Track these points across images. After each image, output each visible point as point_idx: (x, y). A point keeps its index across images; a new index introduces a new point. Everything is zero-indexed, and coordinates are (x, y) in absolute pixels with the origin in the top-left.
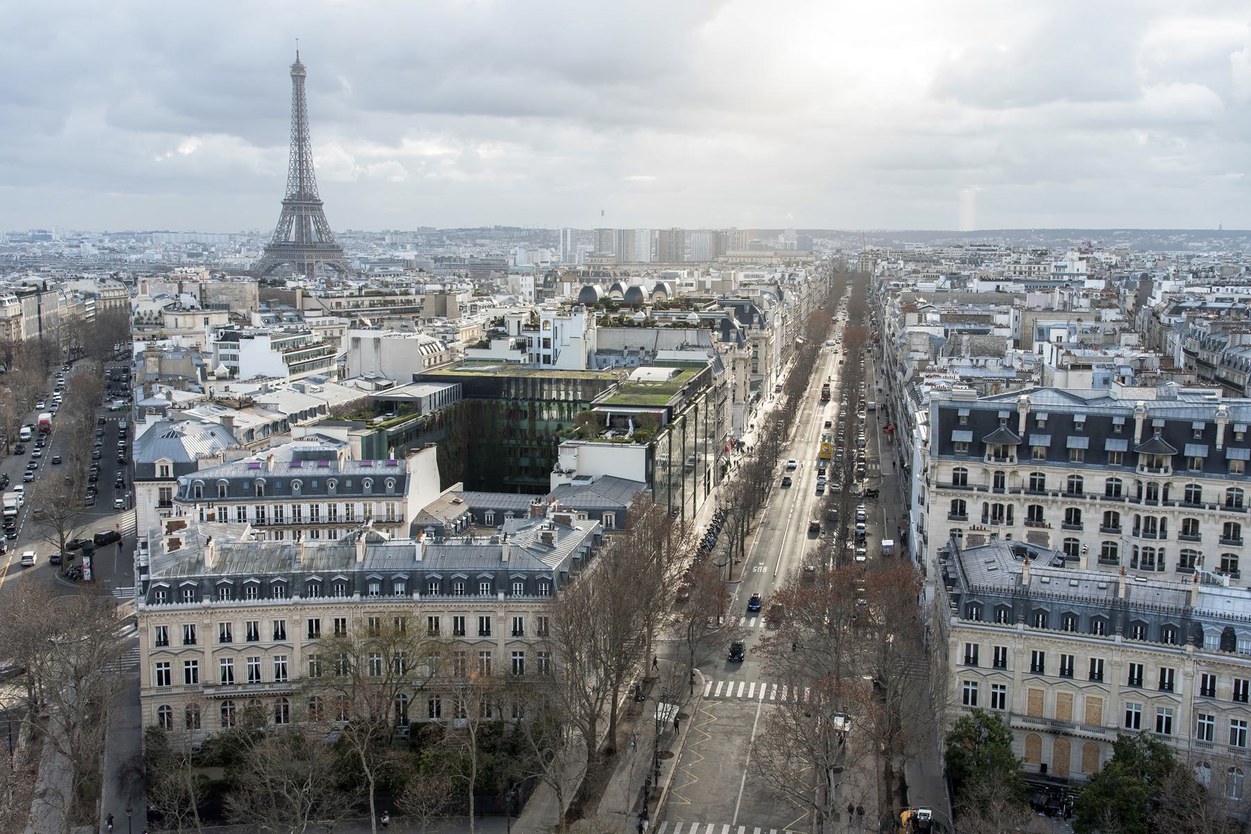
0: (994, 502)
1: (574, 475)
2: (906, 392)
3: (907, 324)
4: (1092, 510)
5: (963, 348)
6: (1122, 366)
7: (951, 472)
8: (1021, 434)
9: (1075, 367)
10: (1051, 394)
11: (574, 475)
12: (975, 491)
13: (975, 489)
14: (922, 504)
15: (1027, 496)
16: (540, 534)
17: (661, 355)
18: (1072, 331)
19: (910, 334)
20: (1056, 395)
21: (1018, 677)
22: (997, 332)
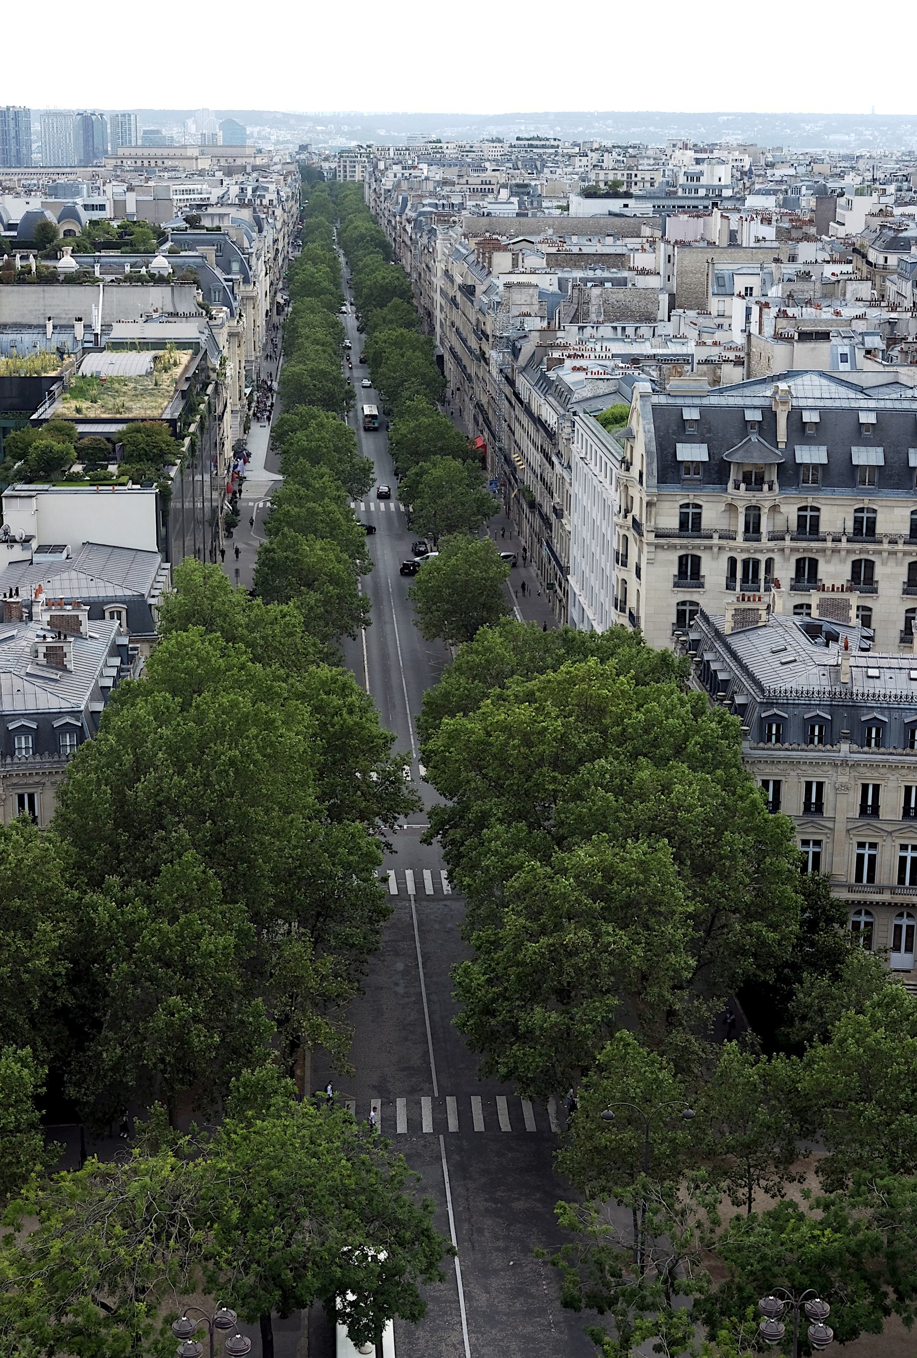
0: (745, 556)
1: (34, 544)
2: (523, 383)
3: (495, 270)
4: (891, 562)
5: (593, 309)
6: (867, 334)
7: (677, 511)
8: (782, 446)
9: (805, 336)
10: (816, 380)
11: (34, 544)
12: (716, 541)
13: (716, 536)
14: (624, 564)
15: (907, 548)
16: (42, 650)
17: (120, 332)
18: (767, 278)
19: (508, 286)
20: (824, 382)
21: (840, 826)
22: (643, 282)
